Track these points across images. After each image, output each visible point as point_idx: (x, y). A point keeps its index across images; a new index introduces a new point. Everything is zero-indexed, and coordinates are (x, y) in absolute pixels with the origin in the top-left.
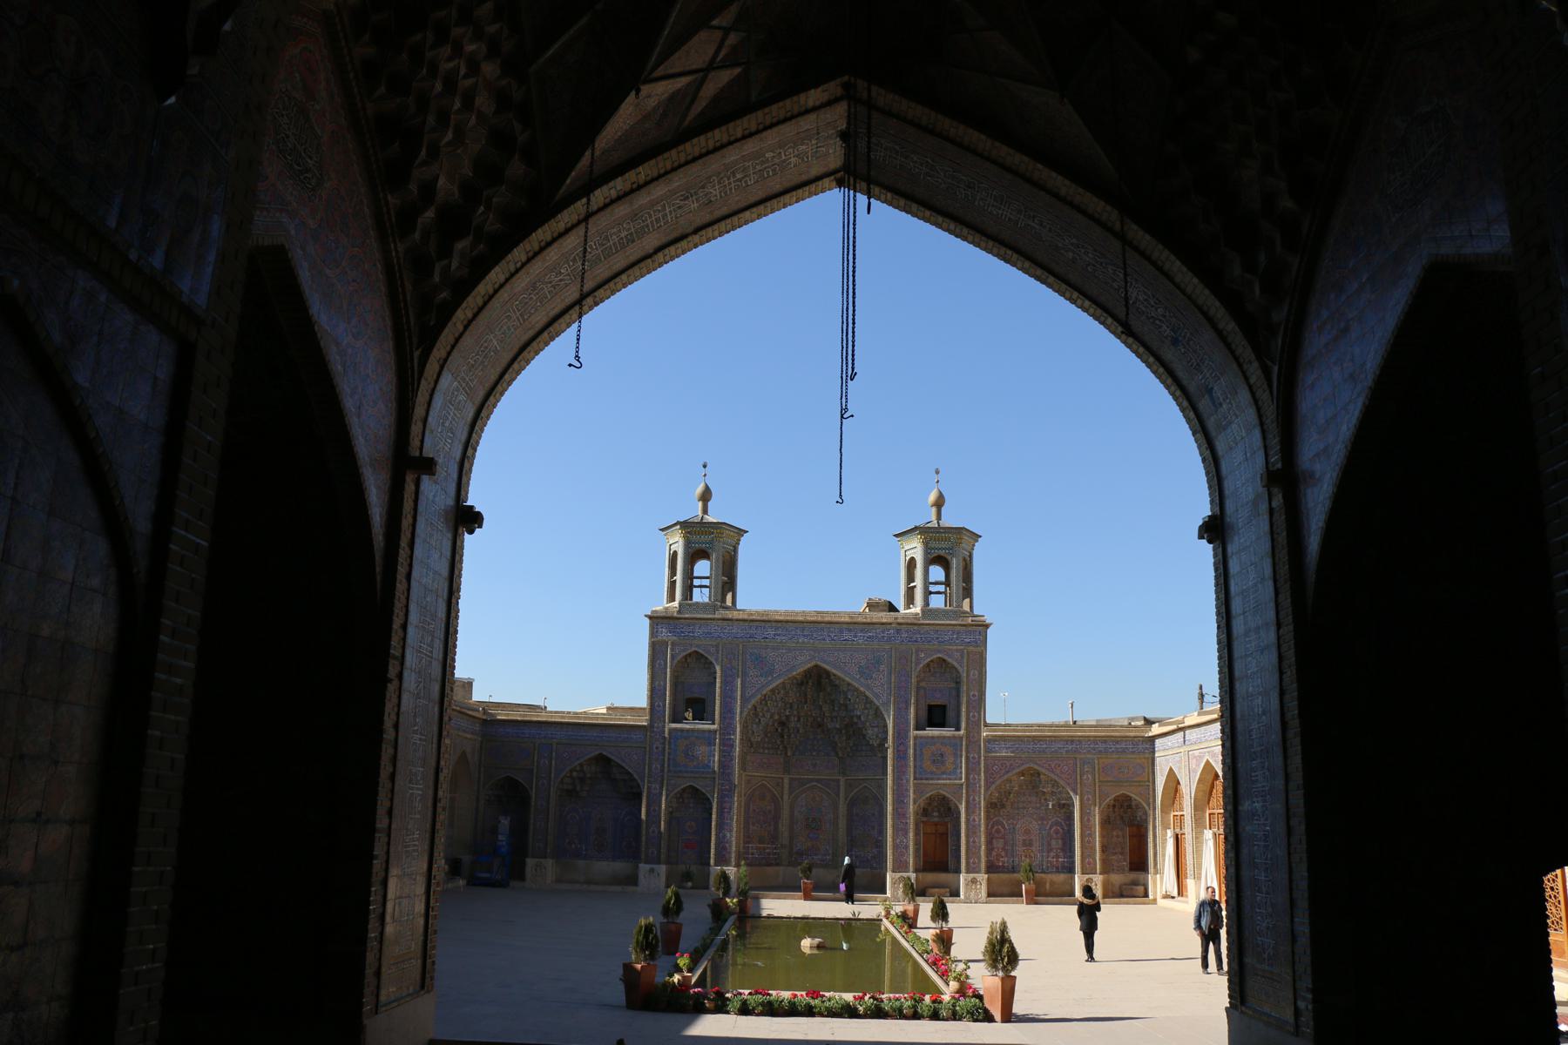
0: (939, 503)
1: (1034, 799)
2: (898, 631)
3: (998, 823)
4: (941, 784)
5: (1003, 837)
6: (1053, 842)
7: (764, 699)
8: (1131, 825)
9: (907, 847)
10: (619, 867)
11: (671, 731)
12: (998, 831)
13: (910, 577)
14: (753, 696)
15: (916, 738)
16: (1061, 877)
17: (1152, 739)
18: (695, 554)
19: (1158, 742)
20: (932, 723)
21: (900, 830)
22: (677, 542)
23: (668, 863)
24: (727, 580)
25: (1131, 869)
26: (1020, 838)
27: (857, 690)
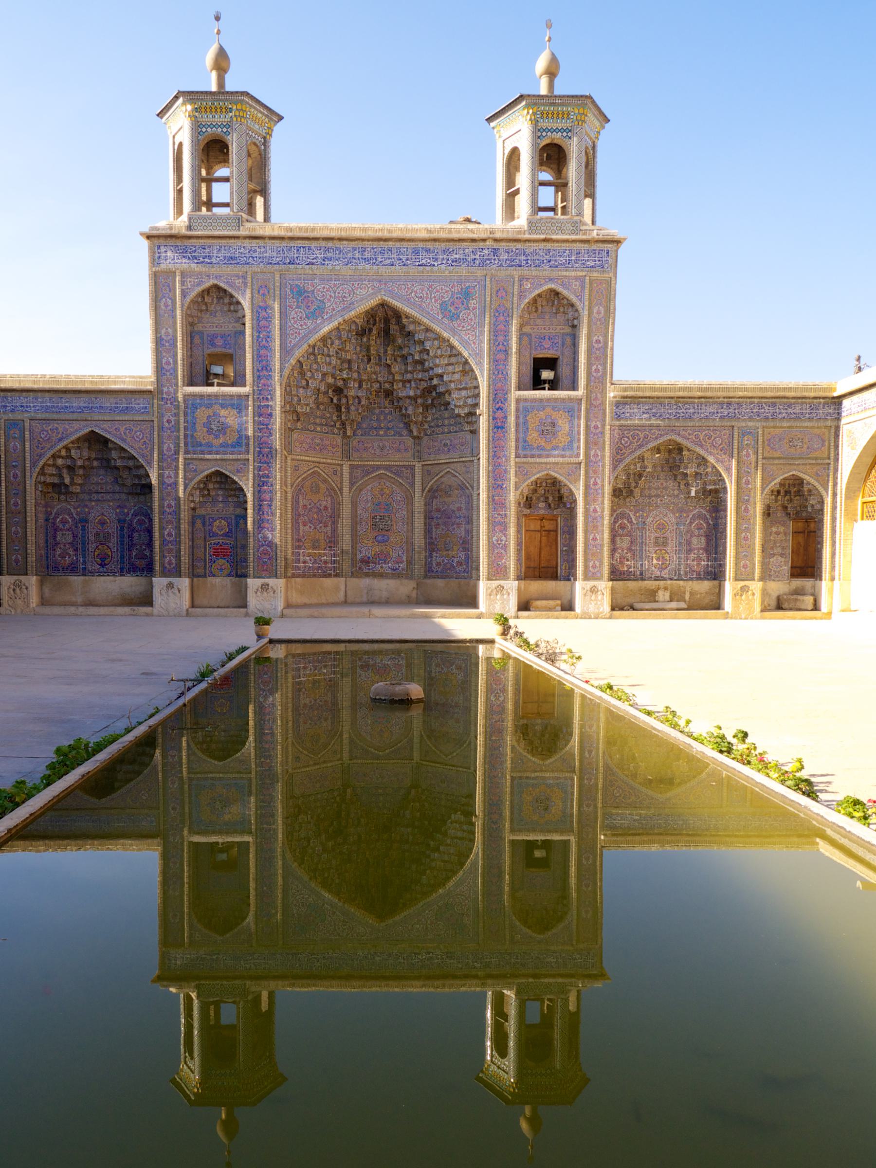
0: (552, 73)
1: (671, 484)
2: (495, 251)
3: (623, 515)
4: (553, 464)
5: (629, 534)
6: (694, 540)
7: (313, 352)
8: (797, 517)
9: (505, 547)
10: (128, 583)
11: (186, 397)
12: (622, 527)
13: (510, 181)
14: (298, 345)
15: (518, 401)
16: (705, 586)
17: (837, 401)
18: (213, 150)
19: (846, 403)
20: (537, 383)
21: (497, 525)
22: (180, 125)
23: (193, 575)
24: (258, 182)
25: (794, 575)
26: (651, 535)
27: (438, 337)
